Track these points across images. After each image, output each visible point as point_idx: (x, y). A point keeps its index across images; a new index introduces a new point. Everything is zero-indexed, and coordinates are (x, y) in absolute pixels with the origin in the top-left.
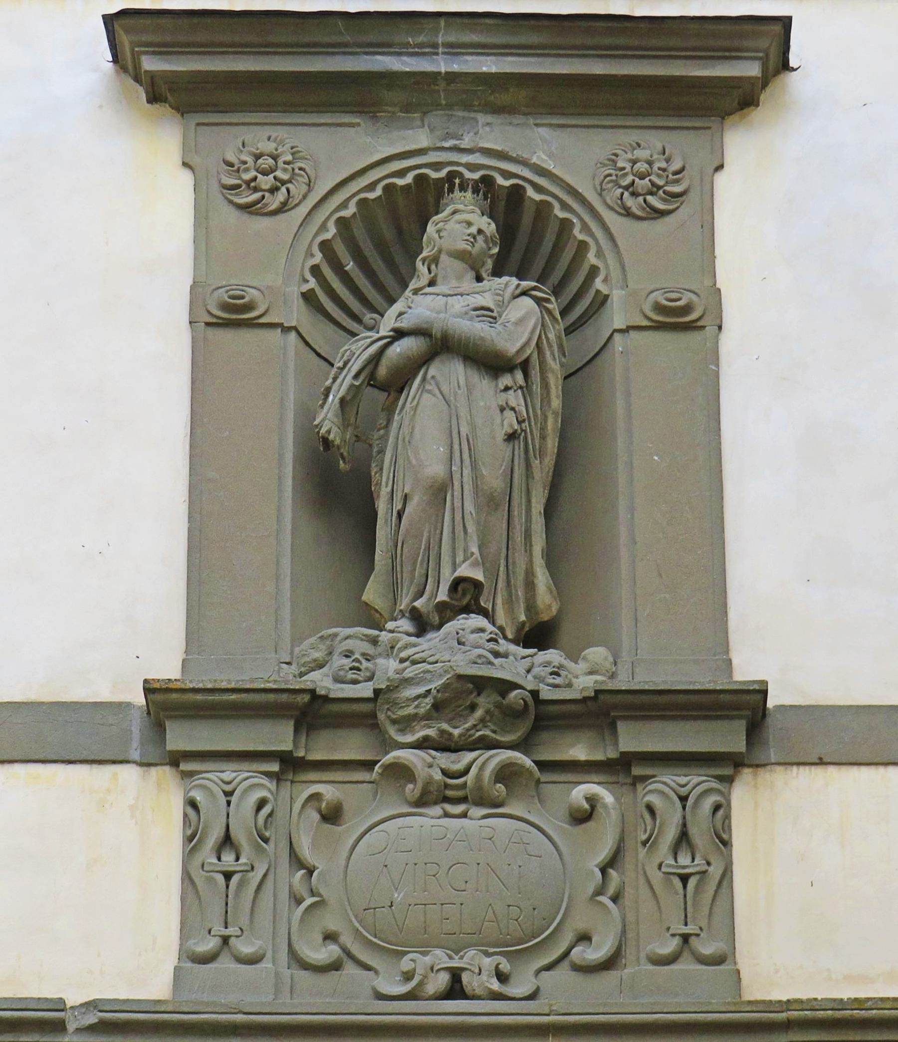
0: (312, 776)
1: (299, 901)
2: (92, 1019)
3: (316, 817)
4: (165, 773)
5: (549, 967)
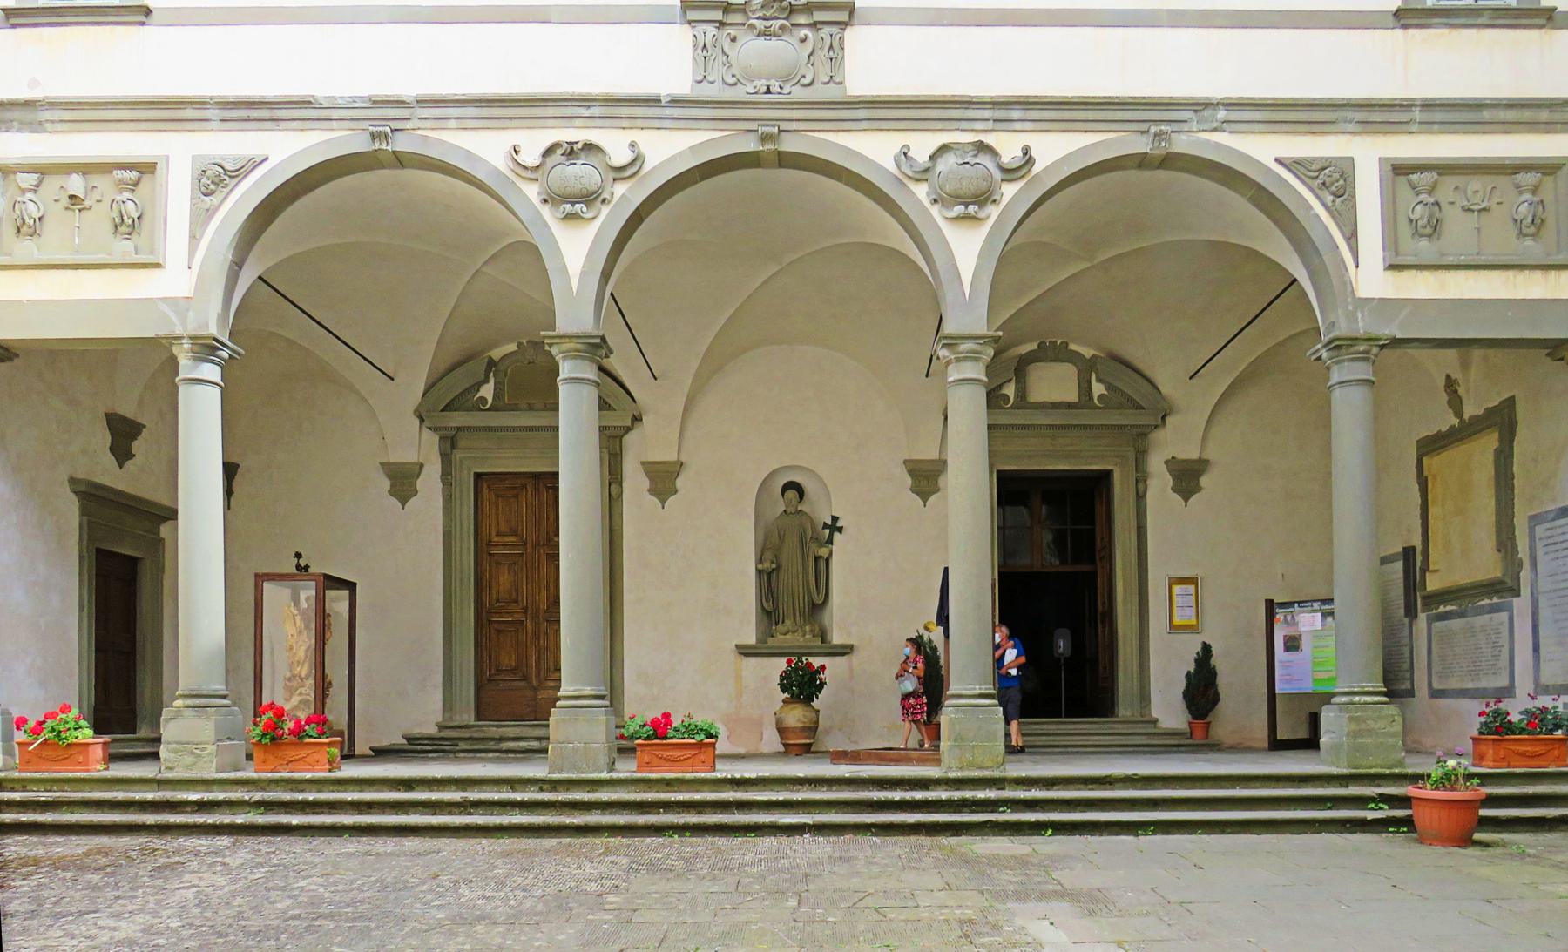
0: (728, 27)
1: (725, 65)
2: (669, 99)
3: (729, 40)
4: (687, 27)
5: (794, 85)
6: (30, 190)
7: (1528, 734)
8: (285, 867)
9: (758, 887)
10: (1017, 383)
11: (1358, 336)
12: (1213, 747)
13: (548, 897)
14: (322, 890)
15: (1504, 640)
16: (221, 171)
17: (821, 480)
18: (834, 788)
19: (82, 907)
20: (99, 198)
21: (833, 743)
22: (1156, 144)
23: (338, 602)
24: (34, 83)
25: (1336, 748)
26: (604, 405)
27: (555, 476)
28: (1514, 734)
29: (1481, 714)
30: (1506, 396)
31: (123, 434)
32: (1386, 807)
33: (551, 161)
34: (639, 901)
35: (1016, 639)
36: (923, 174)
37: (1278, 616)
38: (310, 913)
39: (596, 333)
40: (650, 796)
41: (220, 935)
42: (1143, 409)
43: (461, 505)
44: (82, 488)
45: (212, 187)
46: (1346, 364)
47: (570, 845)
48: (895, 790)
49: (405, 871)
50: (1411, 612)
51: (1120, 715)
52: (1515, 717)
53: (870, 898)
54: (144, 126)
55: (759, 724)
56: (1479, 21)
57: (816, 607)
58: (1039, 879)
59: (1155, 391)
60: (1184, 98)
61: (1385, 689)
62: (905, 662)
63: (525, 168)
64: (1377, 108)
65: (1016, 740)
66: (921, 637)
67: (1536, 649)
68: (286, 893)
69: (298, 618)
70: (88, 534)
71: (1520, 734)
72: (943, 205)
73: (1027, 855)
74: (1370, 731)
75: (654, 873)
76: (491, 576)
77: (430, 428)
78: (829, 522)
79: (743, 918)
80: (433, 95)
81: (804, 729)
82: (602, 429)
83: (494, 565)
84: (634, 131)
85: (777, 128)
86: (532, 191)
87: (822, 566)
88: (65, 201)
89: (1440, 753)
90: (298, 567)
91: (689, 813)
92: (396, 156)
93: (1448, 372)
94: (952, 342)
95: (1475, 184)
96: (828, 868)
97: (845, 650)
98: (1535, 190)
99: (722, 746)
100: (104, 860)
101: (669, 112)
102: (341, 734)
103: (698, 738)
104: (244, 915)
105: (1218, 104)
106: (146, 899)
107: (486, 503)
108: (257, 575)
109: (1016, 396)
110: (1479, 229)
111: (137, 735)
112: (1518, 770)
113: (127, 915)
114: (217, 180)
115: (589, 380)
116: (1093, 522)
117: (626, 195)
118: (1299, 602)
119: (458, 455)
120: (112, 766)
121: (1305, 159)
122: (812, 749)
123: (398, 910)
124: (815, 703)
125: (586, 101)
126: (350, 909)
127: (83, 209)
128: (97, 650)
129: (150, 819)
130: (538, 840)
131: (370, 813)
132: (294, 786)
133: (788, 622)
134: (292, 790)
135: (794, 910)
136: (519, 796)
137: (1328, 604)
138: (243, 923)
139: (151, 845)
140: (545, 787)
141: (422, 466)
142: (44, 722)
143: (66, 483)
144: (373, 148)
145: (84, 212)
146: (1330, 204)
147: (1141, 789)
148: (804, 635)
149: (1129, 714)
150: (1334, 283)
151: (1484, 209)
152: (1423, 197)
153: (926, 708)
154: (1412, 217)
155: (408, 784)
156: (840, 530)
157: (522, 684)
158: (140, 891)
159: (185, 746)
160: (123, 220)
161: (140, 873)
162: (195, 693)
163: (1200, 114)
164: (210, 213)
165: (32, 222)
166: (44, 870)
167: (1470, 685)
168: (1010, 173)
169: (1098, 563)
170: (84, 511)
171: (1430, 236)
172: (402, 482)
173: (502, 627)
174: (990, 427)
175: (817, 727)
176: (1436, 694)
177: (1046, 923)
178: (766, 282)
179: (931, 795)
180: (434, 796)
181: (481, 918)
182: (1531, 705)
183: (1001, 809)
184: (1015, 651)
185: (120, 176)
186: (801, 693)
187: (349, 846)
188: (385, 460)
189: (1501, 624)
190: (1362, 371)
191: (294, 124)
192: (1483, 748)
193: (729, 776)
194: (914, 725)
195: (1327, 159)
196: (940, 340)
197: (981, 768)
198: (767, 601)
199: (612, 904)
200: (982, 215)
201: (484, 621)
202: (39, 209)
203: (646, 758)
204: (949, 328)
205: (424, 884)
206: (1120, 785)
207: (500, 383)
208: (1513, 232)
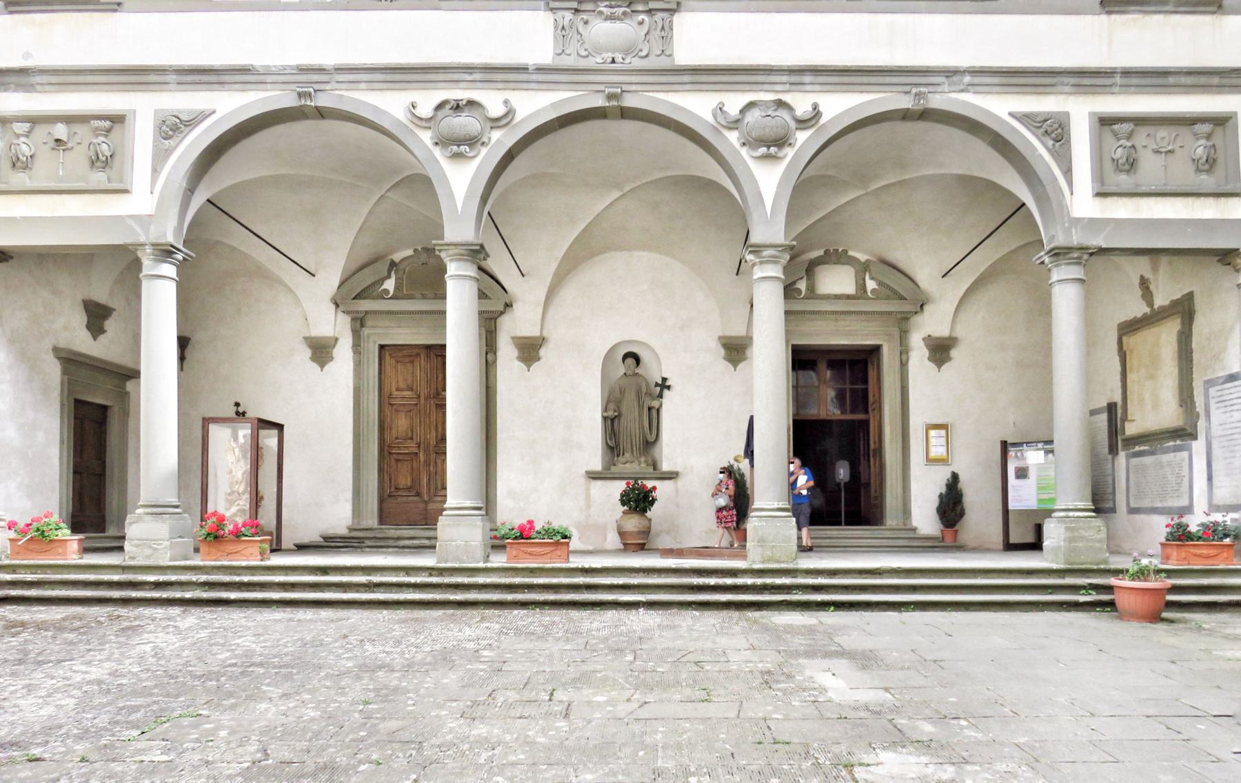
2: (534, 67)
4: (549, 13)
6: (23, 135)
7: (1204, 541)
8: (225, 629)
9: (602, 646)
10: (808, 279)
11: (1073, 246)
12: (959, 548)
13: (436, 653)
14: (254, 646)
15: (1186, 472)
16: (178, 121)
17: (653, 351)
18: (663, 576)
19: (60, 657)
20: (79, 141)
21: (665, 542)
22: (917, 102)
23: (270, 440)
24: (27, 55)
25: (1055, 550)
26: (482, 295)
27: (443, 347)
28: (1192, 540)
29: (1167, 526)
30: (1186, 291)
31: (97, 316)
32: (1094, 593)
33: (441, 114)
34: (508, 656)
35: (806, 468)
36: (735, 124)
37: (1010, 453)
38: (245, 662)
39: (476, 241)
40: (517, 580)
41: (172, 677)
42: (906, 299)
43: (368, 368)
44: (63, 355)
45: (171, 133)
46: (1063, 267)
47: (453, 615)
48: (711, 577)
49: (321, 633)
50: (1113, 450)
51: (888, 524)
52: (1193, 528)
53: (691, 654)
54: (115, 87)
55: (604, 528)
56: (1166, 8)
57: (649, 444)
58: (824, 643)
59: (915, 287)
60: (938, 67)
61: (1093, 507)
62: (719, 484)
63: (421, 119)
64: (1087, 75)
65: (806, 542)
66: (732, 466)
67: (1210, 478)
68: (225, 648)
69: (237, 450)
70: (68, 388)
71: (1197, 540)
72: (750, 147)
73: (814, 625)
74: (1082, 538)
75: (520, 636)
76: (391, 420)
77: (344, 312)
78: (660, 382)
79: (591, 668)
80: (348, 65)
81: (639, 533)
82: (481, 313)
83: (394, 412)
84: (507, 92)
85: (620, 90)
86: (426, 137)
87: (654, 415)
88: (52, 143)
89: (1135, 554)
90: (237, 413)
91: (548, 592)
92: (319, 112)
93: (1142, 273)
94: (757, 249)
95: (1163, 133)
96: (657, 633)
97: (672, 476)
98: (1209, 137)
99: (575, 544)
100: (79, 623)
101: (535, 77)
102: (270, 534)
103: (555, 539)
104: (192, 663)
105: (964, 71)
106: (112, 651)
107: (388, 367)
108: (204, 419)
109: (808, 289)
110: (1165, 166)
111: (106, 534)
112: (1196, 567)
113: (96, 663)
114: (174, 128)
115: (470, 277)
116: (866, 381)
117: (501, 141)
118: (1027, 443)
119: (366, 331)
120: (86, 556)
121: (1031, 113)
122: (646, 547)
123: (315, 661)
124: (649, 514)
125: (469, 69)
126: (276, 660)
127: (66, 149)
128: (75, 472)
129: (116, 594)
130: (428, 611)
131: (293, 591)
132: (232, 571)
133: (627, 455)
134: (231, 574)
135: (631, 662)
136: (412, 580)
137: (1049, 444)
138: (190, 669)
139: (116, 613)
140: (434, 573)
141: (337, 339)
142: (30, 524)
143: (51, 351)
144: (300, 104)
145: (67, 152)
146: (1051, 147)
147: (904, 578)
148: (639, 465)
149: (894, 523)
150: (1054, 206)
151: (1170, 151)
152: (1123, 142)
153: (735, 519)
154: (1114, 157)
155: (324, 570)
156: (669, 387)
157: (416, 499)
158: (108, 646)
159: (143, 542)
160: (98, 157)
161: (108, 633)
162: (153, 504)
163: (951, 79)
164: (168, 152)
165: (25, 159)
166: (29, 630)
167: (1159, 505)
168: (803, 123)
169: (871, 413)
170: (65, 372)
171: (1128, 172)
172: (321, 351)
173: (400, 457)
174: (787, 313)
175: (649, 532)
176: (1133, 511)
177: (829, 674)
178: (611, 204)
179: (739, 581)
180: (345, 579)
181: (381, 667)
182: (1206, 519)
183: (794, 592)
184: (805, 478)
185: (96, 125)
186: (637, 507)
187: (277, 614)
188: (307, 335)
189: (1183, 460)
190: (1075, 272)
191: (237, 86)
192: (1169, 550)
193: (580, 567)
194: (725, 530)
195: (1048, 113)
196: (747, 248)
197: (778, 562)
198: (610, 439)
199: (486, 657)
200: (780, 155)
201: (386, 453)
202: (30, 149)
203: (514, 553)
204: (755, 239)
205: (336, 642)
206: (888, 575)
207: (399, 278)
208: (1192, 168)
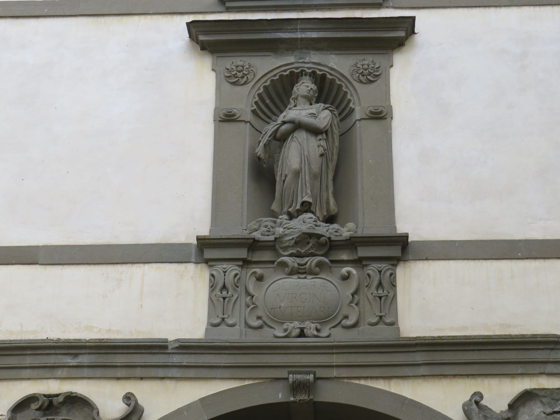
0: (253, 266)
1: (248, 306)
2: (177, 345)
3: (255, 279)
5: (334, 327)
85: (312, 376)
101: (176, 359)
